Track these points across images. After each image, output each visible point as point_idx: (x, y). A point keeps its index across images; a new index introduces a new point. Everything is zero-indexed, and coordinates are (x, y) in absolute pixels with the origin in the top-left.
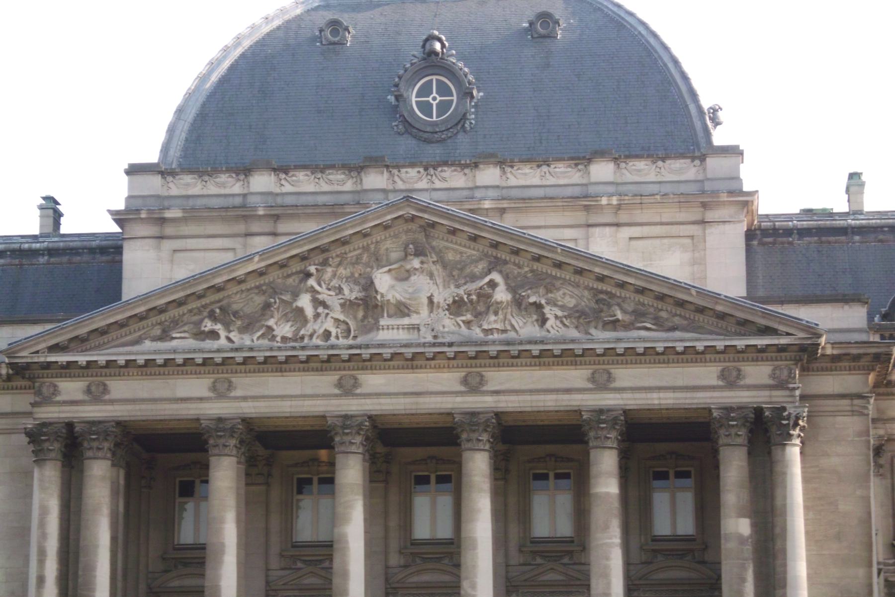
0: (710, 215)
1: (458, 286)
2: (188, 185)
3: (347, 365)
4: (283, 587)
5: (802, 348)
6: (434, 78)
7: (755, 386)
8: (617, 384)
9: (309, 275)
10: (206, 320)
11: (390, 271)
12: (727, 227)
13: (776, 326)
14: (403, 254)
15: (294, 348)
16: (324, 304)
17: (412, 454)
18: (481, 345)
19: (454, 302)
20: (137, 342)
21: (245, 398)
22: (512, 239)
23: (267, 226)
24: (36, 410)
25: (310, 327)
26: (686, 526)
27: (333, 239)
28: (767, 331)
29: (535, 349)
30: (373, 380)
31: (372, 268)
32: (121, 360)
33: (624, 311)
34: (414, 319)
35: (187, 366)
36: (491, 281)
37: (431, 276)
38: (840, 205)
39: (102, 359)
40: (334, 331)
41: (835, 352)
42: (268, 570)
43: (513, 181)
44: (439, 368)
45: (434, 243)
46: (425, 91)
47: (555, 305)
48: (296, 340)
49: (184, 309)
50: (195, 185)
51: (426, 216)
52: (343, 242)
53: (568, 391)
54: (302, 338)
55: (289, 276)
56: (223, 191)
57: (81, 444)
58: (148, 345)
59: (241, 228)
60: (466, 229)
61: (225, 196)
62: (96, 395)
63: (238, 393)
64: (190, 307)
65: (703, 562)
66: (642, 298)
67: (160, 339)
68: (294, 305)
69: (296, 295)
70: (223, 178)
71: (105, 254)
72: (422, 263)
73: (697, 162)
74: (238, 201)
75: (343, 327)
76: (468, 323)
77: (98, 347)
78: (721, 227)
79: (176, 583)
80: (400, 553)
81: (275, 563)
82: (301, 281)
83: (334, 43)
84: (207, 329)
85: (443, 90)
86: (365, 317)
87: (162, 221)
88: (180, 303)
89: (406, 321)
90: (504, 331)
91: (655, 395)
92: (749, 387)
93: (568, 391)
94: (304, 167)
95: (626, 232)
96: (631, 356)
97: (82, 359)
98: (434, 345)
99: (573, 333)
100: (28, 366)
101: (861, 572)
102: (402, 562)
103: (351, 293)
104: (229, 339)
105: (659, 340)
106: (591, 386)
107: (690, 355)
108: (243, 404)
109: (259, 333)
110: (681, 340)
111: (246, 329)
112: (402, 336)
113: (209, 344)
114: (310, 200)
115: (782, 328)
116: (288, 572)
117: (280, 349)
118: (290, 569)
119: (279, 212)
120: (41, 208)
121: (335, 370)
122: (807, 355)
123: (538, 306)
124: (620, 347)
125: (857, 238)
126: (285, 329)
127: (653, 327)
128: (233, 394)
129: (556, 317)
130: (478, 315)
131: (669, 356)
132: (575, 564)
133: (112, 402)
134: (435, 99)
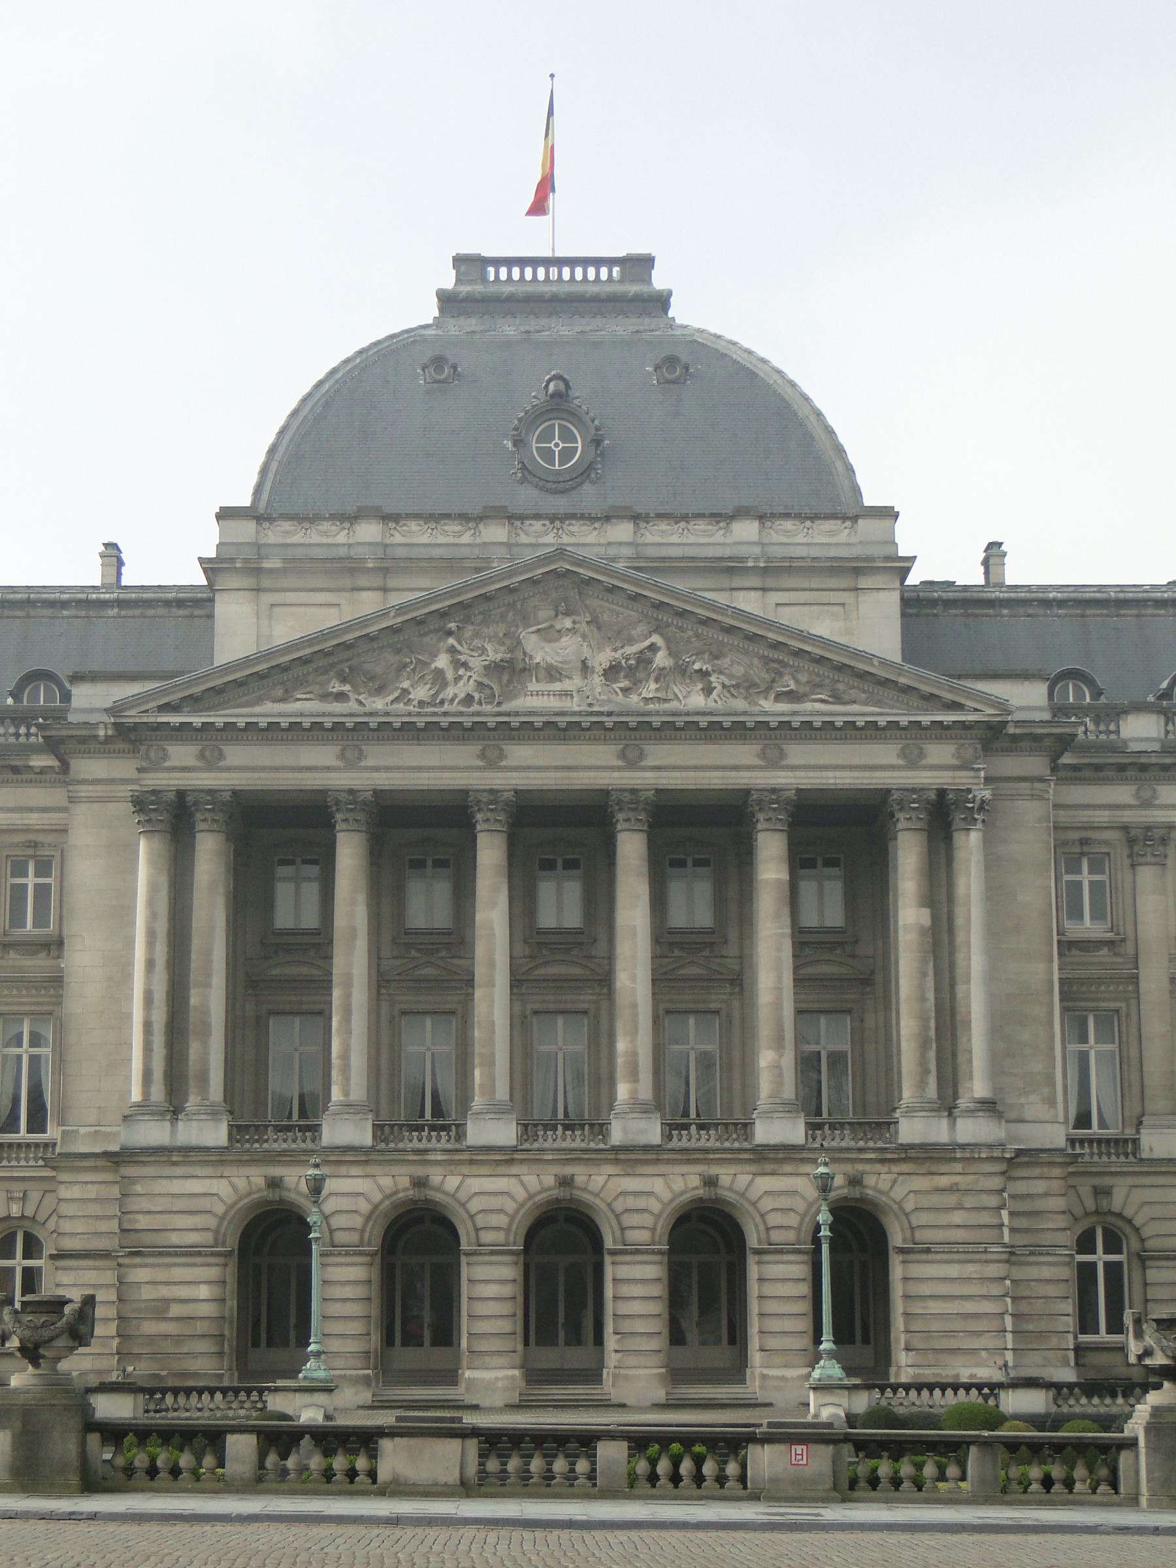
0: (864, 582)
1: (615, 650)
2: (287, 532)
4: (397, 978)
5: (988, 726)
6: (557, 423)
7: (940, 768)
8: (790, 761)
9: (450, 633)
10: (334, 681)
11: (538, 631)
12: (882, 594)
13: (963, 701)
14: (552, 613)
15: (435, 714)
16: (464, 664)
17: (562, 834)
18: (643, 715)
19: (611, 667)
20: (259, 701)
21: (377, 769)
22: (677, 599)
23: (377, 581)
24: (143, 775)
25: (450, 692)
26: (835, 917)
27: (477, 594)
28: (955, 706)
29: (703, 721)
30: (520, 753)
31: (517, 627)
32: (241, 722)
33: (797, 681)
34: (567, 685)
35: (315, 732)
36: (652, 644)
37: (584, 637)
38: (970, 575)
39: (220, 721)
40: (476, 696)
41: (1018, 731)
42: (379, 958)
43: (649, 538)
44: (593, 740)
45: (588, 602)
46: (547, 436)
47: (721, 673)
48: (435, 705)
49: (310, 668)
50: (294, 533)
51: (581, 571)
52: (486, 598)
53: (736, 768)
54: (442, 702)
55: (426, 634)
56: (325, 540)
57: (192, 815)
58: (269, 707)
59: (348, 582)
60: (625, 586)
61: (329, 545)
62: (211, 762)
63: (369, 762)
64: (314, 665)
65: (854, 956)
66: (817, 668)
67: (282, 700)
68: (433, 666)
69: (434, 656)
70: (326, 526)
71: (189, 607)
72: (574, 622)
73: (848, 523)
74: (343, 552)
75: (487, 691)
76: (625, 691)
78: (875, 594)
79: (276, 972)
80: (525, 942)
81: (386, 953)
82: (439, 640)
83: (439, 382)
84: (334, 690)
85: (567, 436)
86: (510, 682)
87: (258, 572)
88: (304, 661)
89: (557, 686)
90: (666, 701)
91: (830, 774)
92: (932, 768)
93: (736, 768)
94: (417, 516)
95: (774, 597)
96: (809, 731)
97: (197, 720)
98: (592, 714)
99: (740, 704)
100: (136, 727)
101: (1041, 967)
102: (527, 953)
103: (495, 653)
104: (360, 703)
105: (840, 713)
106: (760, 762)
107: (872, 731)
108: (375, 775)
109: (392, 697)
110: (860, 711)
111: (380, 690)
112: (554, 703)
113: (337, 707)
114: (424, 553)
115: (969, 703)
116: (399, 962)
117: (419, 714)
118: (404, 958)
119: (388, 567)
120: (102, 556)
121: (478, 739)
122: (994, 736)
123: (703, 674)
124: (796, 721)
125: (1005, 612)
126: (421, 693)
127: (831, 700)
128: (363, 764)
129: (724, 686)
130: (637, 683)
131: (851, 731)
132: (716, 957)
133: (229, 769)
134: (557, 445)
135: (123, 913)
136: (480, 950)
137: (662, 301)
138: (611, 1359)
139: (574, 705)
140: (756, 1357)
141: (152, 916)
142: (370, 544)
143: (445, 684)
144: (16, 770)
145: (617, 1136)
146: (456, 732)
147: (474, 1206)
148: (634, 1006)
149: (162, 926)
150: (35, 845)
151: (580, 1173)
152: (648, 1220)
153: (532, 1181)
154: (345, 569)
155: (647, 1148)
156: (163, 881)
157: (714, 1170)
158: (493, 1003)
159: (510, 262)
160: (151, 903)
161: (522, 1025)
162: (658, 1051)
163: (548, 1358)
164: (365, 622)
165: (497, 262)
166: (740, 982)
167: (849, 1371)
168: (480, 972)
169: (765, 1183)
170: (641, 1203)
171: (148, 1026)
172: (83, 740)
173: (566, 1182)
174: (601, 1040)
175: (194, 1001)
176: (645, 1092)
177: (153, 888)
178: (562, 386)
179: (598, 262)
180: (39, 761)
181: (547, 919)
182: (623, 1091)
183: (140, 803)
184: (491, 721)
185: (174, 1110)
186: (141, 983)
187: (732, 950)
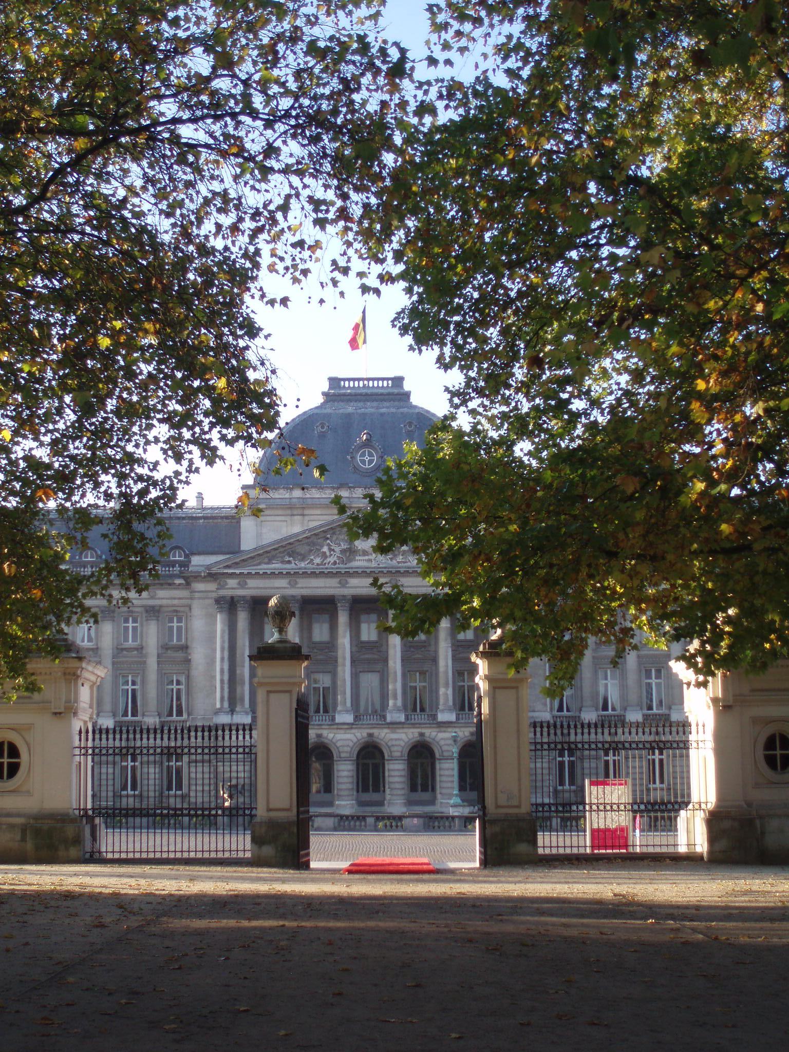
3: (344, 575)
20: (259, 564)
23: (300, 512)
39: (246, 572)
46: (363, 455)
59: (289, 512)
62: (242, 585)
67: (268, 563)
69: (322, 546)
74: (288, 501)
77: (243, 567)
85: (370, 455)
88: (275, 549)
97: (238, 571)
103: (344, 546)
111: (303, 560)
113: (287, 566)
126: (318, 560)
134: (367, 458)
135: (211, 639)
136: (340, 653)
137: (407, 395)
138: (388, 797)
139: (374, 564)
140: (439, 796)
141: (223, 642)
143: (326, 557)
144: (170, 584)
145: (389, 719)
146: (331, 575)
147: (339, 744)
148: (395, 672)
149: (226, 645)
150: (176, 611)
151: (376, 732)
152: (400, 749)
153: (359, 735)
154: (290, 508)
155: (400, 723)
156: (226, 629)
157: (423, 731)
158: (345, 671)
159: (349, 380)
160: (222, 637)
161: (355, 676)
162: (404, 686)
163: (366, 797)
164: (297, 534)
165: (344, 380)
166: (435, 660)
167: (463, 801)
168: (340, 660)
169: (441, 735)
170: (397, 743)
171: (222, 681)
172: (196, 577)
173: (371, 735)
174: (384, 682)
175: (238, 672)
176: (399, 703)
177: (223, 631)
179: (383, 379)
180: (178, 581)
181: (364, 637)
182: (391, 702)
183: (218, 601)
184: (343, 571)
185: (232, 711)
186: (220, 666)
187: (432, 648)
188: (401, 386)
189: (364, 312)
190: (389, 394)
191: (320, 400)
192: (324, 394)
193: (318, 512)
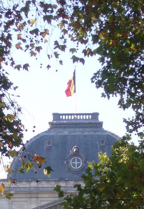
23: (35, 195)
46: (74, 161)
56: (24, 186)
59: (29, 196)
70: (24, 183)
74: (28, 189)
85: (78, 161)
134: (76, 163)
137: (101, 124)
142: (34, 187)
159: (65, 115)
165: (62, 115)
178: (77, 149)
179: (86, 114)
188: (97, 119)
189: (74, 73)
190: (89, 123)
191: (48, 127)
192: (50, 123)
193: (47, 196)
